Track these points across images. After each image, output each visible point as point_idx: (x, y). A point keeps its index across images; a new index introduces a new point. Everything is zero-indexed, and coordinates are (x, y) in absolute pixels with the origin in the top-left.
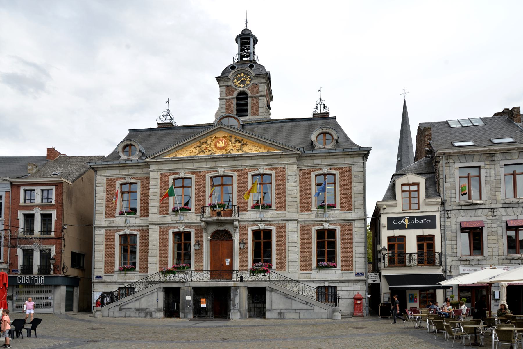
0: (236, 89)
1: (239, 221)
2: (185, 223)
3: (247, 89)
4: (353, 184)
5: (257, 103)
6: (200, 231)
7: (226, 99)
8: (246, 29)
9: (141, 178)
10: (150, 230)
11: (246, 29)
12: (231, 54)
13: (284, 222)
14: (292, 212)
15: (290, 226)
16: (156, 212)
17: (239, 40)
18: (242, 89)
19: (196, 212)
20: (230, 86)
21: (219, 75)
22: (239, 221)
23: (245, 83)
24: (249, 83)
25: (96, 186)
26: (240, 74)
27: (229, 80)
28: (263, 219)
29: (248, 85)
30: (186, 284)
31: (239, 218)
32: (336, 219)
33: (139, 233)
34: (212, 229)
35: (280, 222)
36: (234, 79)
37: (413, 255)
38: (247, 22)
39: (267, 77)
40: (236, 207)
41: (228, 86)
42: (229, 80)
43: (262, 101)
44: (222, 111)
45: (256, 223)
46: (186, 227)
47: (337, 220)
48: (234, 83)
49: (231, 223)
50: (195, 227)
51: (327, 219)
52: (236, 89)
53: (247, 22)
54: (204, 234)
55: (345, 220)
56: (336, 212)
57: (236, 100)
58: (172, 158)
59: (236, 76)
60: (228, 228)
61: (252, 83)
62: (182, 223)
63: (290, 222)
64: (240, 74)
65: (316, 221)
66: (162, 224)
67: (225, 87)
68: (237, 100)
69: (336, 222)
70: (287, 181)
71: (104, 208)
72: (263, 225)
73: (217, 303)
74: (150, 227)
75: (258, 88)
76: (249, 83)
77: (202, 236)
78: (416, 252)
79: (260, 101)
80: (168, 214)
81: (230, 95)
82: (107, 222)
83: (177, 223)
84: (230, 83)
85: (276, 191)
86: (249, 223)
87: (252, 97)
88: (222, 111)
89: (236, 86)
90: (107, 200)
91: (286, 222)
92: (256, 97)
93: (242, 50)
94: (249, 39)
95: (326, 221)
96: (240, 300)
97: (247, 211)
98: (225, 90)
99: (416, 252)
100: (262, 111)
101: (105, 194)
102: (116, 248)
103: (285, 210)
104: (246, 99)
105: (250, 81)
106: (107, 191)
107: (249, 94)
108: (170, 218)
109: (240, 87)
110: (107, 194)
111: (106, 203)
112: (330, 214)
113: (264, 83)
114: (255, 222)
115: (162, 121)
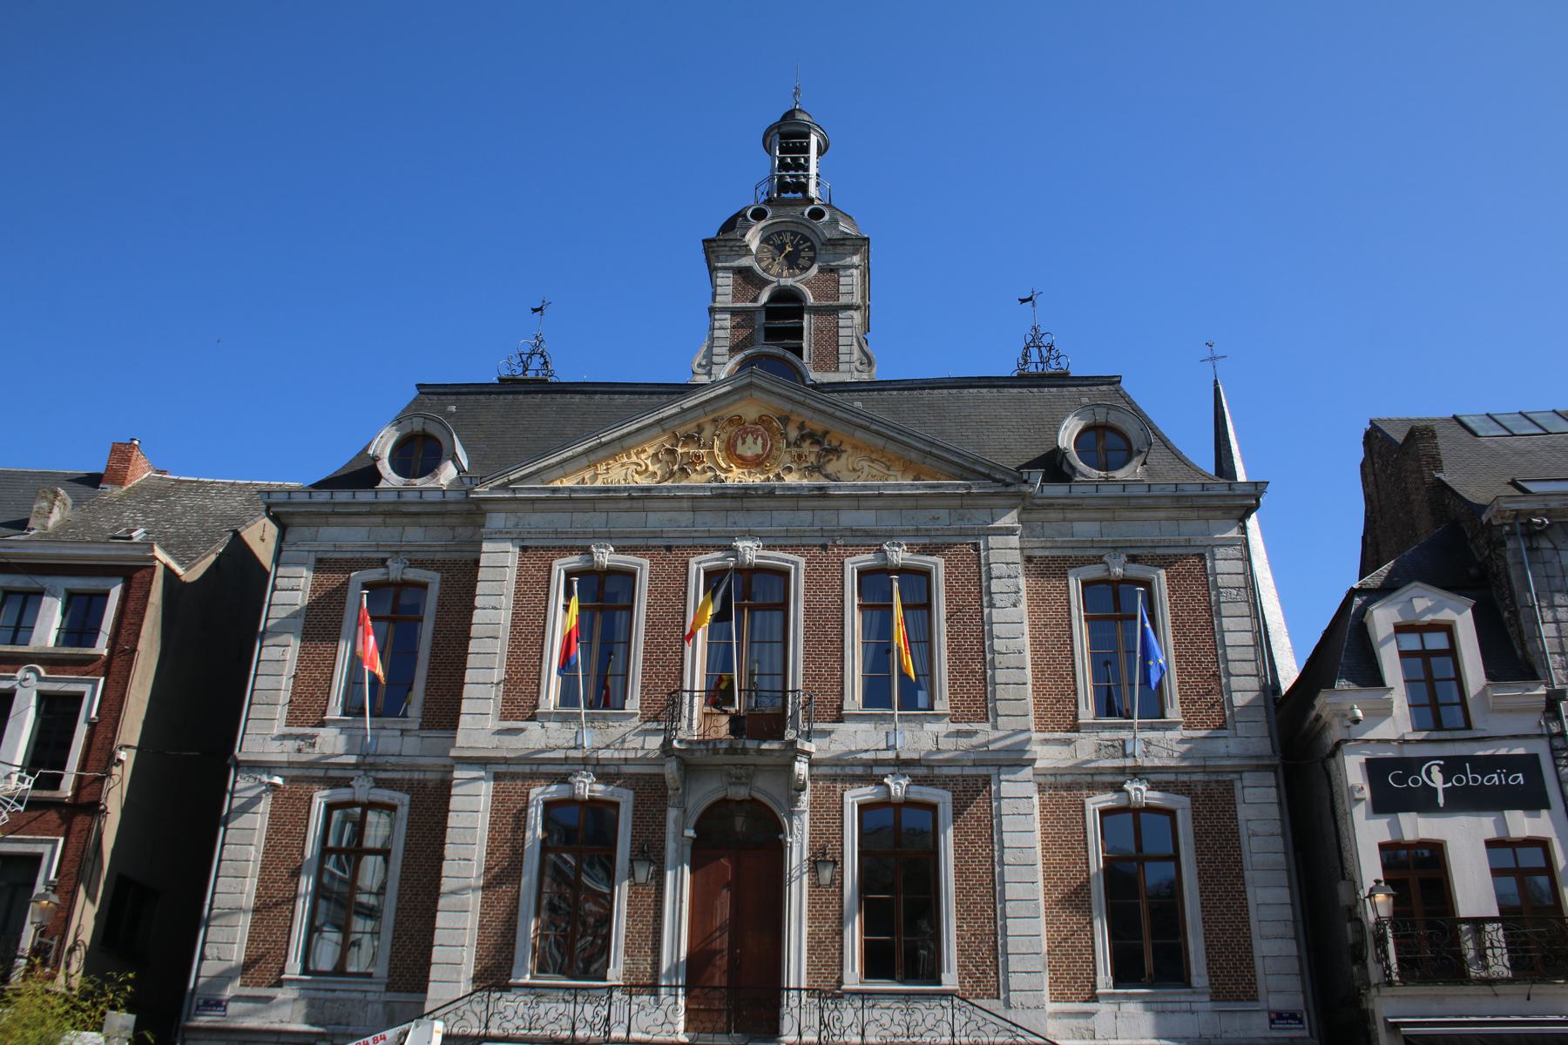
7: (734, 312)
18: (788, 282)
21: (713, 235)
27: (747, 251)
28: (903, 756)
34: (705, 793)
37: (1488, 927)
43: (849, 323)
45: (877, 771)
48: (759, 261)
52: (766, 283)
54: (672, 814)
55: (1204, 769)
56: (1169, 734)
60: (765, 789)
62: (585, 762)
68: (768, 317)
72: (904, 782)
78: (1496, 913)
79: (841, 323)
87: (816, 310)
91: (992, 771)
93: (783, 166)
94: (807, 136)
95: (1137, 773)
97: (840, 718)
98: (730, 281)
99: (1496, 913)
100: (847, 358)
104: (798, 313)
111: (301, 659)
112: (1148, 743)
114: (868, 772)
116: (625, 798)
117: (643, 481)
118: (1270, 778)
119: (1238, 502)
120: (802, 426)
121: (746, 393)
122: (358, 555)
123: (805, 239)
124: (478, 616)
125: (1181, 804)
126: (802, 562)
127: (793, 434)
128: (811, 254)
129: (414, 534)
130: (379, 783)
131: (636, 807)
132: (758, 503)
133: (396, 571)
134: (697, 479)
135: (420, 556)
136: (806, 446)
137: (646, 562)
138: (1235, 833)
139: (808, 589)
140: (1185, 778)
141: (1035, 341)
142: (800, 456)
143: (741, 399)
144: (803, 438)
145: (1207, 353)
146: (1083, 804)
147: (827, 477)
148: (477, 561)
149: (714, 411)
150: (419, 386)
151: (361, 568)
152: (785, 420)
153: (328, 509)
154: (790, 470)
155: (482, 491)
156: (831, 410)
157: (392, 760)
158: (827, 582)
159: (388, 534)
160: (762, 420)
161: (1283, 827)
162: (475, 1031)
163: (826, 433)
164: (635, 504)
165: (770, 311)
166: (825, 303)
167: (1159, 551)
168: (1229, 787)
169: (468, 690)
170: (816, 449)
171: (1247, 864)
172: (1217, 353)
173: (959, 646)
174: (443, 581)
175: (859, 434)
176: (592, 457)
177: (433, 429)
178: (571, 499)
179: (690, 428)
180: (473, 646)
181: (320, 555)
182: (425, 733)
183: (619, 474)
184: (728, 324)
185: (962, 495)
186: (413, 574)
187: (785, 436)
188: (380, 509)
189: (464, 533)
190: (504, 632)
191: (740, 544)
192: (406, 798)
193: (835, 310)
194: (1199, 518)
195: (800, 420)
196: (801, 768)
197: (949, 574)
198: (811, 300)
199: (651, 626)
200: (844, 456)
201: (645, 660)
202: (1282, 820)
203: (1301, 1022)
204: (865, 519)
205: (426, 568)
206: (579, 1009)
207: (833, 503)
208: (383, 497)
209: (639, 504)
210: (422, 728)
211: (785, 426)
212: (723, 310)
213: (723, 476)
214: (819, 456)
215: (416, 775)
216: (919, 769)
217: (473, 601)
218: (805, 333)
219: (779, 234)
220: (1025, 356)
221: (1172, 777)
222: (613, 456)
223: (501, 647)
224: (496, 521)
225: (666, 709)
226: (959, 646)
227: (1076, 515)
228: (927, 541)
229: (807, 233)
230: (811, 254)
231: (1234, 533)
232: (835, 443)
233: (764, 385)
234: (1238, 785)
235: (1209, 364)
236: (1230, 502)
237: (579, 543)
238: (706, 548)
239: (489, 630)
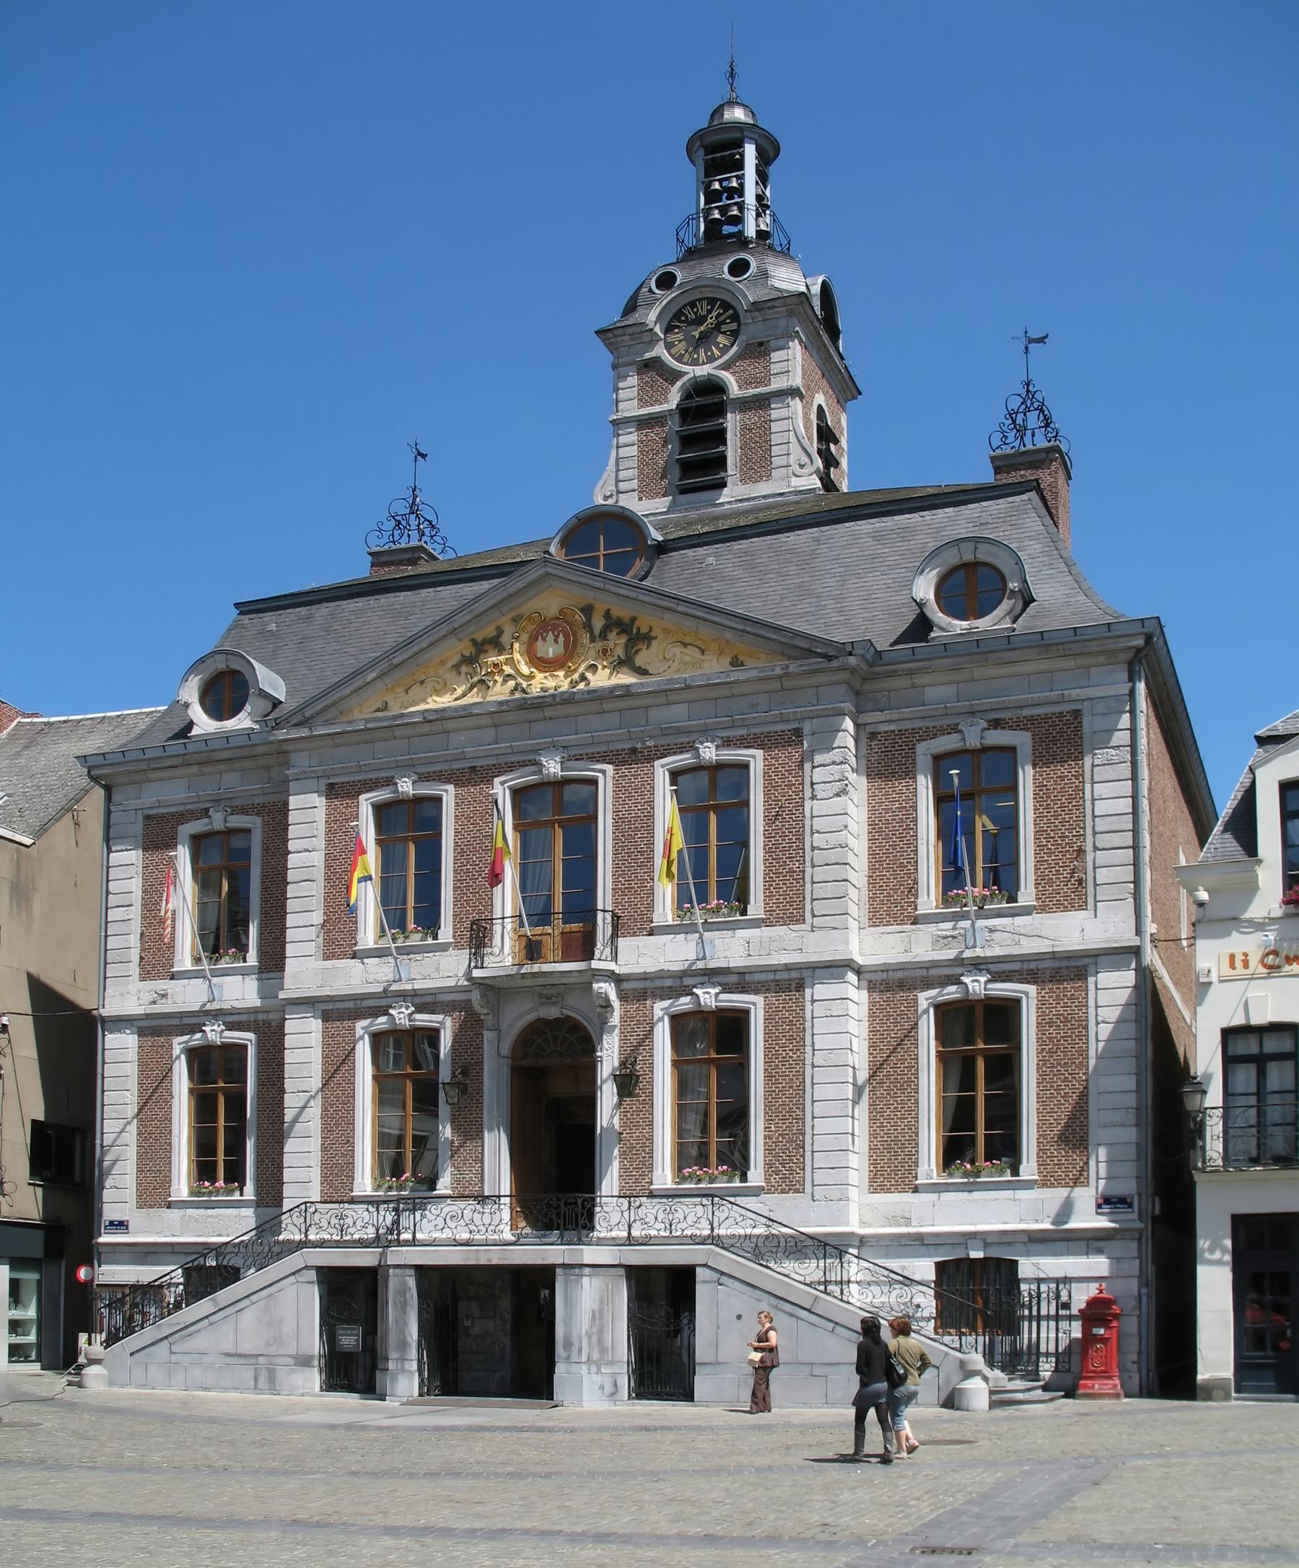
18: (702, 371)
30: (397, 1256)
33: (251, 1036)
40: (609, 917)
48: (669, 346)
52: (680, 374)
58: (367, 721)
70: (808, 793)
73: (491, 1337)
77: (480, 1047)
81: (658, 402)
82: (146, 998)
85: (768, 836)
96: (594, 1317)
102: (175, 1102)
104: (720, 410)
109: (695, 363)
110: (145, 880)
115: (379, 543)
120: (607, 615)
122: (182, 808)
123: (726, 306)
124: (292, 860)
127: (598, 623)
128: (734, 326)
132: (559, 711)
133: (217, 821)
135: (238, 802)
136: (612, 636)
139: (616, 798)
148: (286, 804)
149: (513, 609)
151: (187, 821)
154: (593, 668)
156: (633, 595)
162: (297, 1237)
163: (633, 619)
165: (685, 412)
166: (752, 391)
170: (623, 640)
173: (777, 845)
174: (265, 824)
175: (668, 616)
177: (236, 665)
186: (237, 821)
187: (588, 626)
190: (319, 874)
193: (762, 402)
195: (606, 607)
198: (735, 390)
199: (460, 851)
200: (654, 643)
201: (455, 889)
203: (1130, 1206)
204: (676, 714)
206: (381, 1219)
207: (640, 702)
208: (192, 748)
212: (627, 421)
214: (627, 648)
216: (739, 980)
218: (729, 436)
219: (692, 304)
223: (317, 889)
225: (477, 936)
226: (777, 845)
229: (727, 297)
230: (734, 326)
232: (644, 630)
233: (561, 574)
237: (384, 774)
239: (304, 874)
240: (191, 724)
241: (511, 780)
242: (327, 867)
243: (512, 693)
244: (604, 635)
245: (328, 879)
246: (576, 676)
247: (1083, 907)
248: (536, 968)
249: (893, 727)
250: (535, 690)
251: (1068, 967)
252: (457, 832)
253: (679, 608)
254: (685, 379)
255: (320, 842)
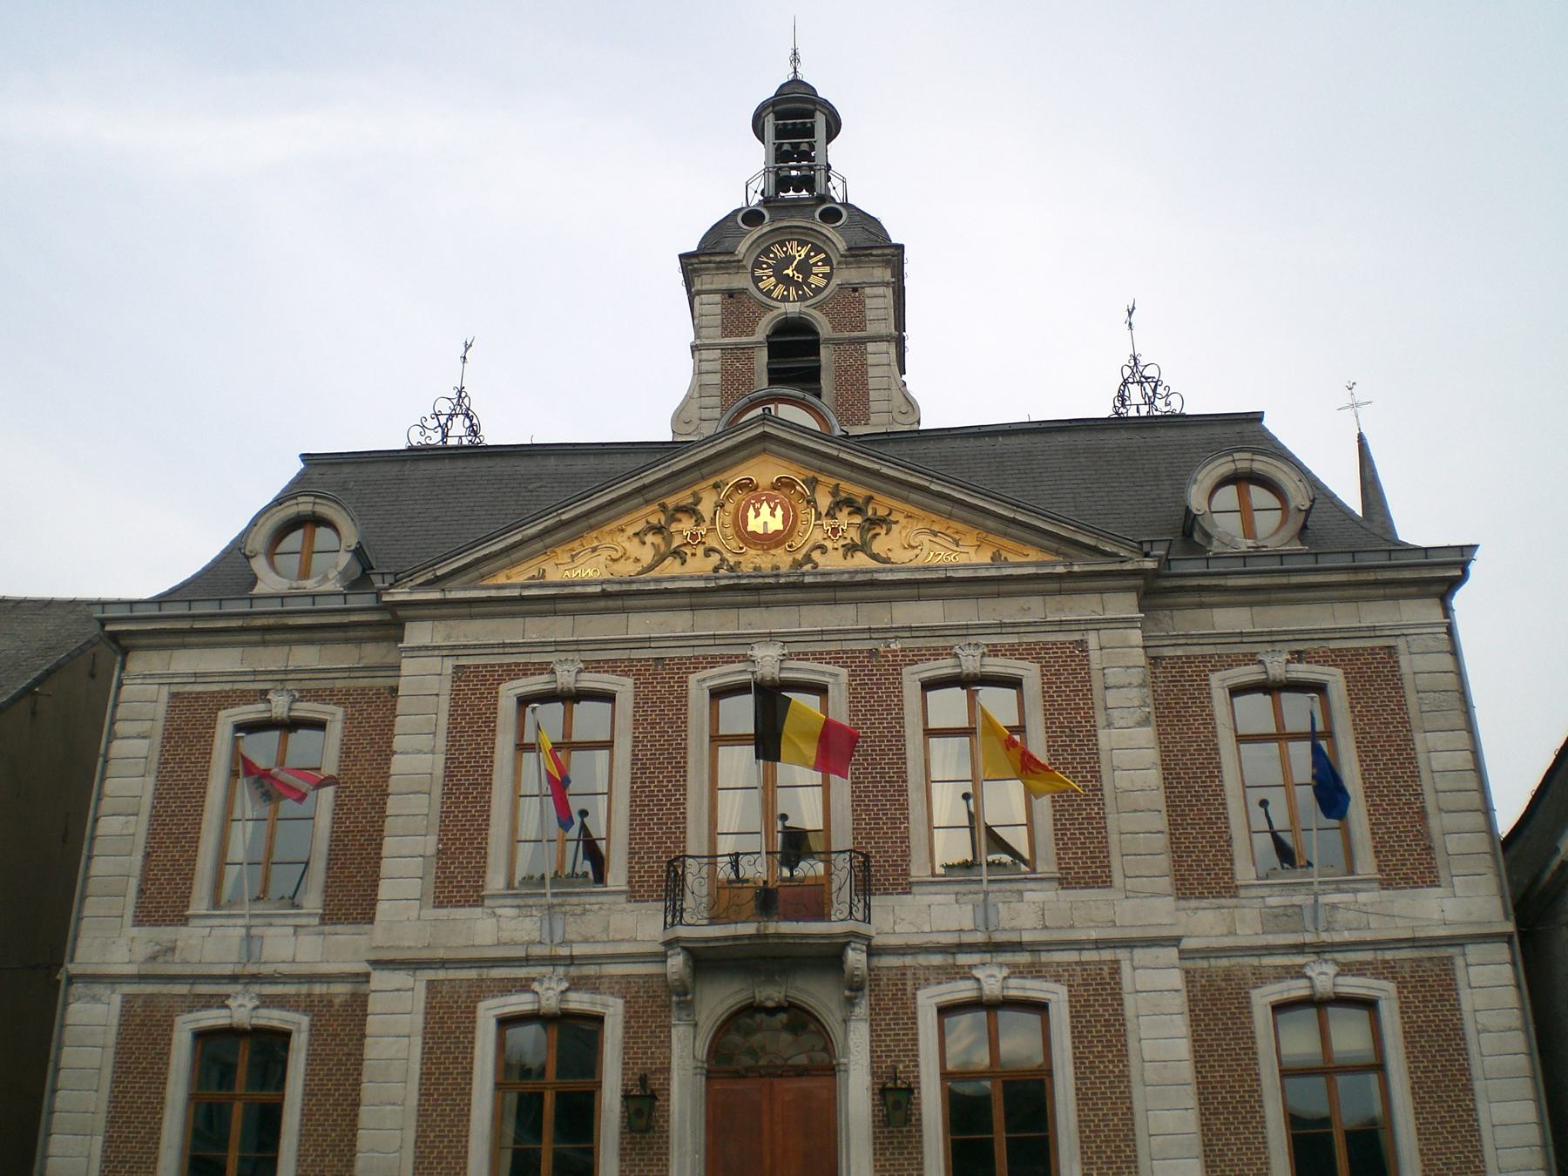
0: (770, 308)
1: (872, 951)
2: (572, 960)
3: (818, 306)
4: (1418, 737)
5: (863, 367)
6: (655, 1004)
8: (796, 82)
9: (348, 693)
10: (374, 1003)
11: (796, 82)
12: (738, 171)
13: (1107, 955)
14: (1140, 899)
15: (1145, 979)
16: (413, 888)
17: (770, 123)
18: (792, 308)
19: (635, 894)
20: (743, 291)
22: (872, 951)
23: (797, 282)
24: (822, 283)
25: (113, 736)
26: (782, 244)
28: (999, 937)
29: (818, 290)
31: (870, 930)
32: (1368, 936)
35: (1088, 956)
36: (758, 264)
38: (795, 57)
39: (895, 256)
41: (730, 294)
42: (738, 266)
43: (884, 359)
44: (707, 401)
45: (963, 959)
46: (576, 984)
47: (1376, 945)
49: (828, 958)
50: (624, 987)
51: (1326, 937)
53: (795, 57)
55: (1413, 942)
57: (765, 352)
59: (766, 251)
61: (835, 281)
62: (553, 961)
63: (1139, 954)
64: (782, 244)
65: (1270, 950)
66: (444, 964)
67: (718, 298)
69: (1367, 956)
71: (138, 859)
74: (380, 979)
75: (862, 302)
76: (822, 283)
79: (871, 359)
80: (479, 901)
83: (526, 961)
84: (741, 281)
86: (923, 960)
87: (837, 343)
88: (707, 401)
89: (768, 293)
90: (154, 817)
91: (1122, 954)
92: (852, 341)
93: (781, 156)
94: (811, 115)
95: (1320, 949)
98: (718, 309)
100: (884, 406)
101: (150, 781)
103: (1104, 881)
104: (813, 347)
105: (828, 277)
106: (163, 763)
107: (824, 328)
108: (491, 928)
109: (785, 299)
111: (152, 833)
112: (1334, 906)
113: (886, 284)
116: (613, 1011)
117: (626, 569)
118: (1502, 951)
119: (1439, 573)
120: (835, 491)
121: (758, 447)
124: (398, 764)
125: (1385, 991)
126: (844, 672)
127: (824, 501)
128: (827, 269)
129: (306, 656)
130: (267, 1002)
131: (627, 1026)
134: (699, 565)
136: (843, 518)
137: (629, 682)
138: (1458, 1031)
140: (1388, 955)
141: (1136, 373)
142: (835, 530)
143: (751, 456)
144: (837, 505)
145: (1346, 399)
146: (1247, 997)
147: (874, 557)
150: (305, 457)
152: (812, 483)
153: (185, 625)
155: (400, 595)
157: (285, 969)
158: (880, 702)
159: (270, 658)
160: (784, 484)
161: (1524, 1017)
163: (870, 499)
164: (611, 603)
167: (1333, 645)
168: (1447, 965)
169: (386, 866)
170: (858, 520)
171: (1476, 1071)
172: (1359, 398)
174: (348, 718)
176: (549, 541)
178: (522, 599)
179: (684, 498)
180: (393, 805)
181: (175, 689)
182: (327, 929)
183: (584, 566)
184: (717, 366)
185: (1059, 576)
187: (811, 502)
188: (258, 622)
189: (373, 653)
191: (759, 652)
192: (305, 1021)
194: (1385, 598)
196: (855, 958)
197: (1046, 684)
202: (1522, 1009)
205: (323, 701)
209: (619, 603)
210: (325, 919)
211: (813, 491)
213: (732, 560)
215: (318, 989)
217: (389, 743)
220: (1122, 397)
221: (1367, 956)
222: (578, 536)
224: (418, 633)
227: (1216, 598)
228: (1014, 640)
230: (827, 269)
231: (1436, 614)
232: (882, 512)
234: (1459, 962)
235: (1350, 412)
236: (1426, 574)
237: (535, 659)
238: (713, 662)
240: (254, 580)
241: (712, 678)
242: (449, 774)
243: (716, 569)
244: (831, 514)
245: (447, 793)
246: (799, 556)
247: (1434, 884)
248: (773, 927)
249: (1179, 652)
250: (747, 568)
251: (1430, 959)
252: (636, 741)
253: (934, 487)
254: (776, 312)
255: (441, 742)
